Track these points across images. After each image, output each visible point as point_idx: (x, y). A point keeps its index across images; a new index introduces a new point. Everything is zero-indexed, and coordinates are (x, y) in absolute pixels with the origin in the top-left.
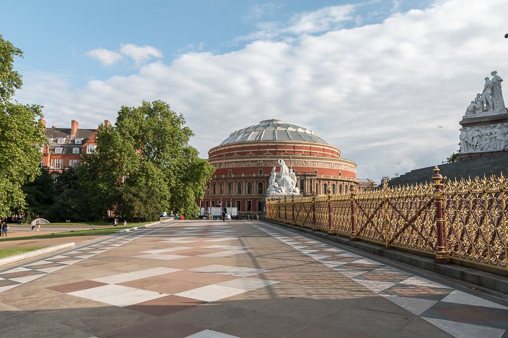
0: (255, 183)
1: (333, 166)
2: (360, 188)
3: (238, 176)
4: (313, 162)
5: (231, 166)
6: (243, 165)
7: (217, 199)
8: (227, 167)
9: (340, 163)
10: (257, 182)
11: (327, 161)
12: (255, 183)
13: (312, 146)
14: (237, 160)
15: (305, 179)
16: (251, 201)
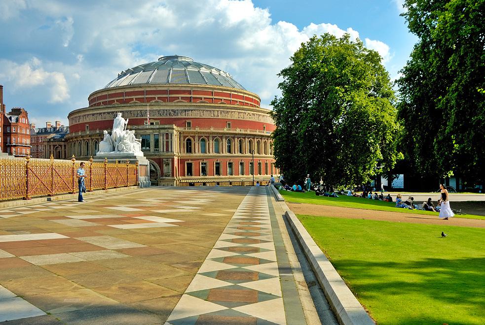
1: (216, 113)
3: (93, 132)
4: (185, 111)
5: (88, 120)
6: (99, 119)
15: (159, 132)
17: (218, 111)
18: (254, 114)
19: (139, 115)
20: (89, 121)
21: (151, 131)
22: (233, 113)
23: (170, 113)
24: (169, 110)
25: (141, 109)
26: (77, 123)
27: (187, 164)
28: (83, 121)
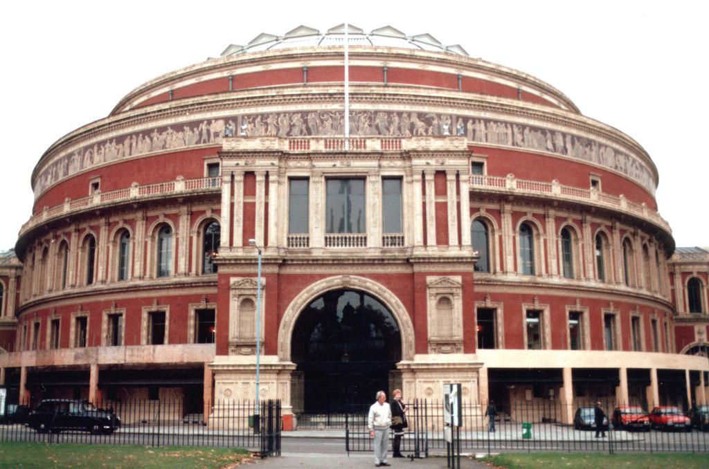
0: (184, 222)
1: (559, 141)
2: (672, 275)
3: (119, 198)
4: (466, 119)
5: (99, 160)
6: (142, 150)
7: (46, 313)
8: (88, 166)
9: (592, 137)
10: (193, 216)
11: (533, 122)
12: (184, 222)
13: (466, 73)
14: (121, 132)
16: (167, 309)
17: (564, 135)
18: (641, 166)
19: (296, 131)
20: (102, 164)
21: (374, 163)
22: (602, 150)
23: (412, 127)
24: (409, 114)
25: (305, 107)
26: (61, 178)
27: (479, 310)
28: (82, 167)
